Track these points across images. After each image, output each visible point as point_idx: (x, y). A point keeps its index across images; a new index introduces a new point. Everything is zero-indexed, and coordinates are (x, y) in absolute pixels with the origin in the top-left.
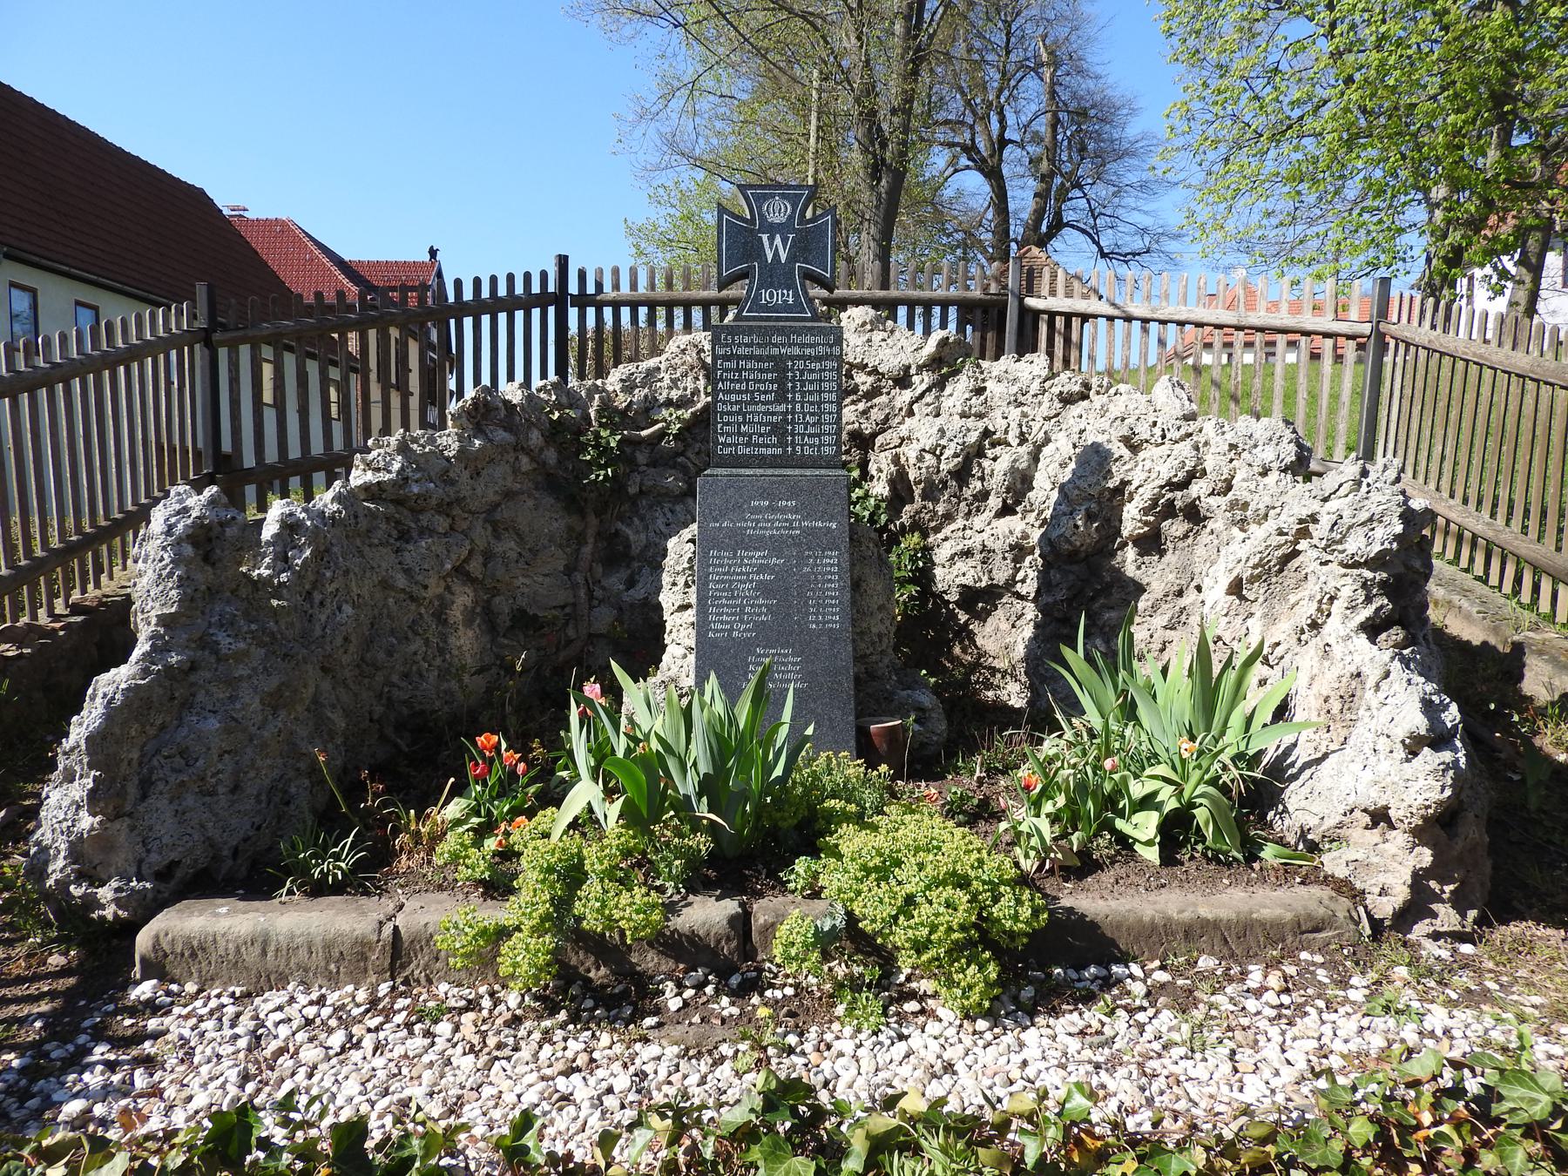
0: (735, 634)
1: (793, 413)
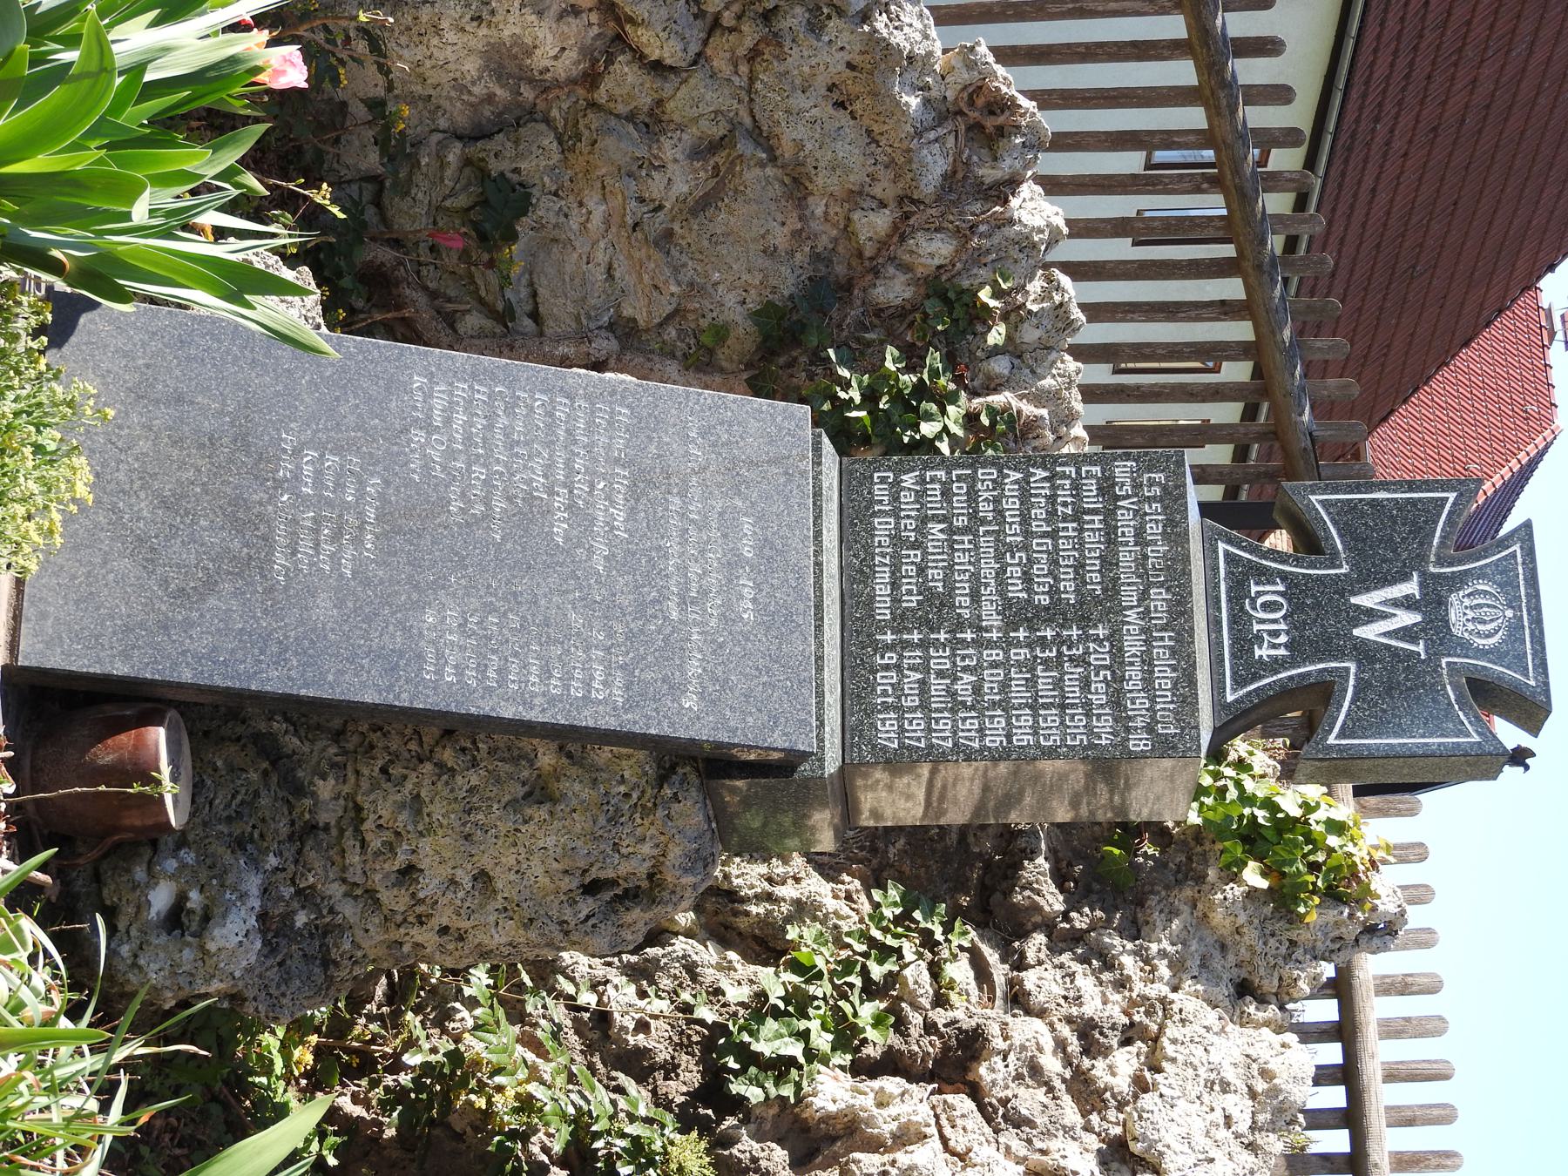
0: (418, 436)
1: (979, 644)
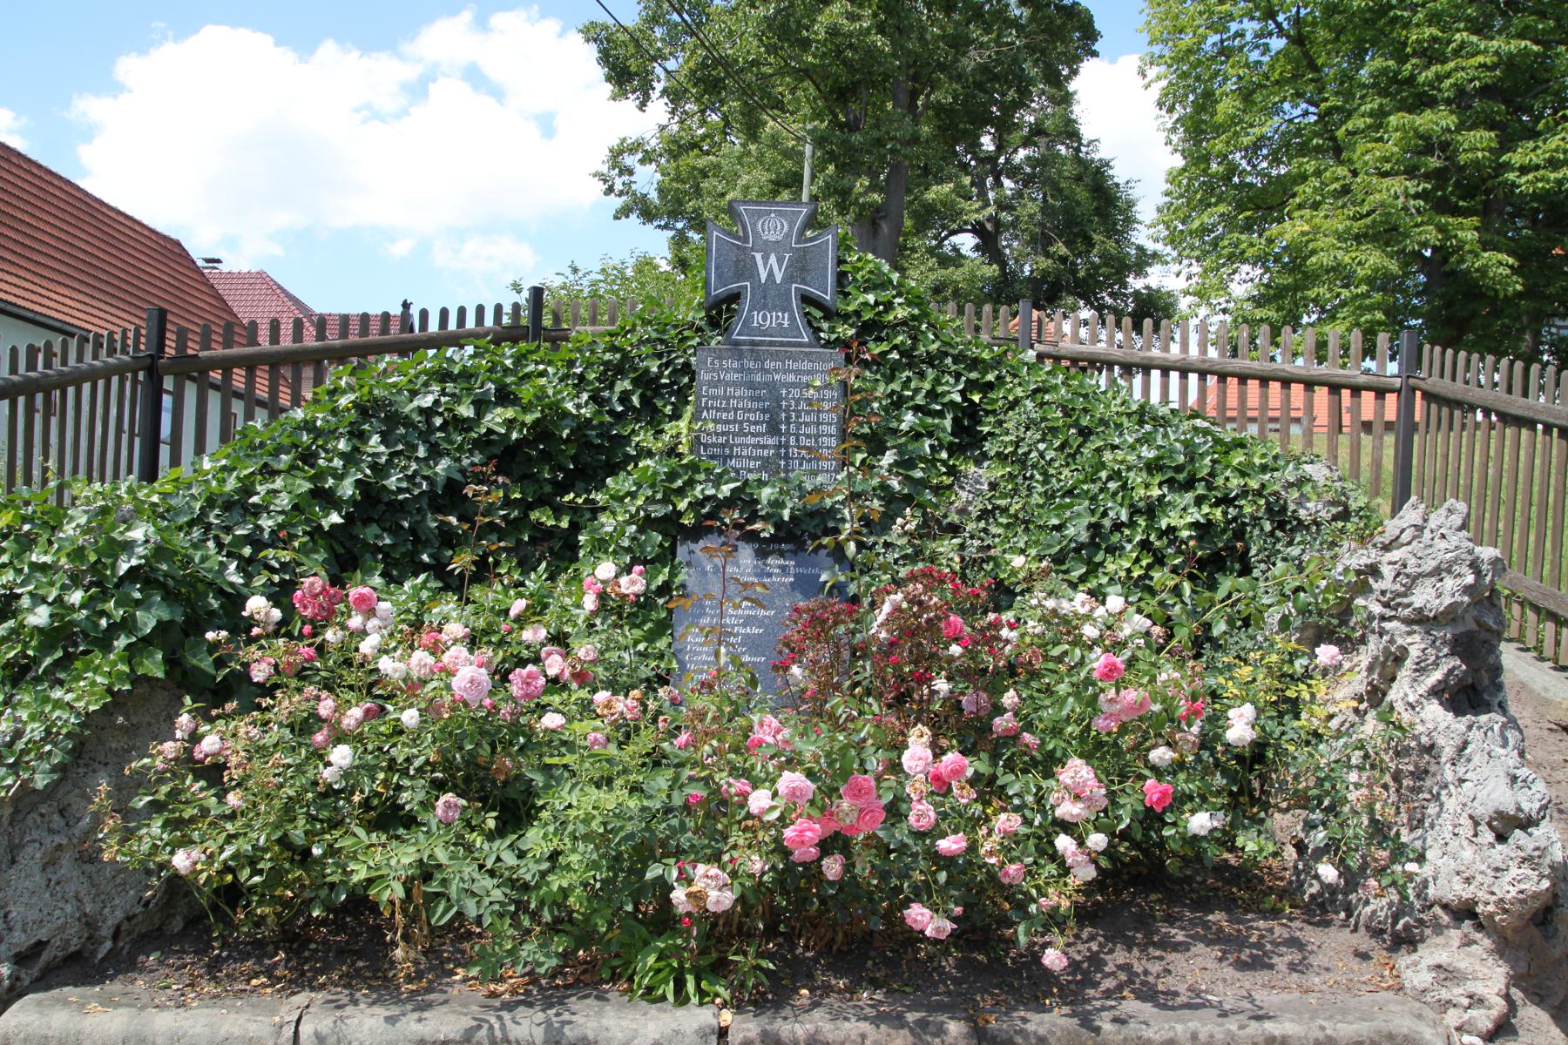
1: (787, 447)
